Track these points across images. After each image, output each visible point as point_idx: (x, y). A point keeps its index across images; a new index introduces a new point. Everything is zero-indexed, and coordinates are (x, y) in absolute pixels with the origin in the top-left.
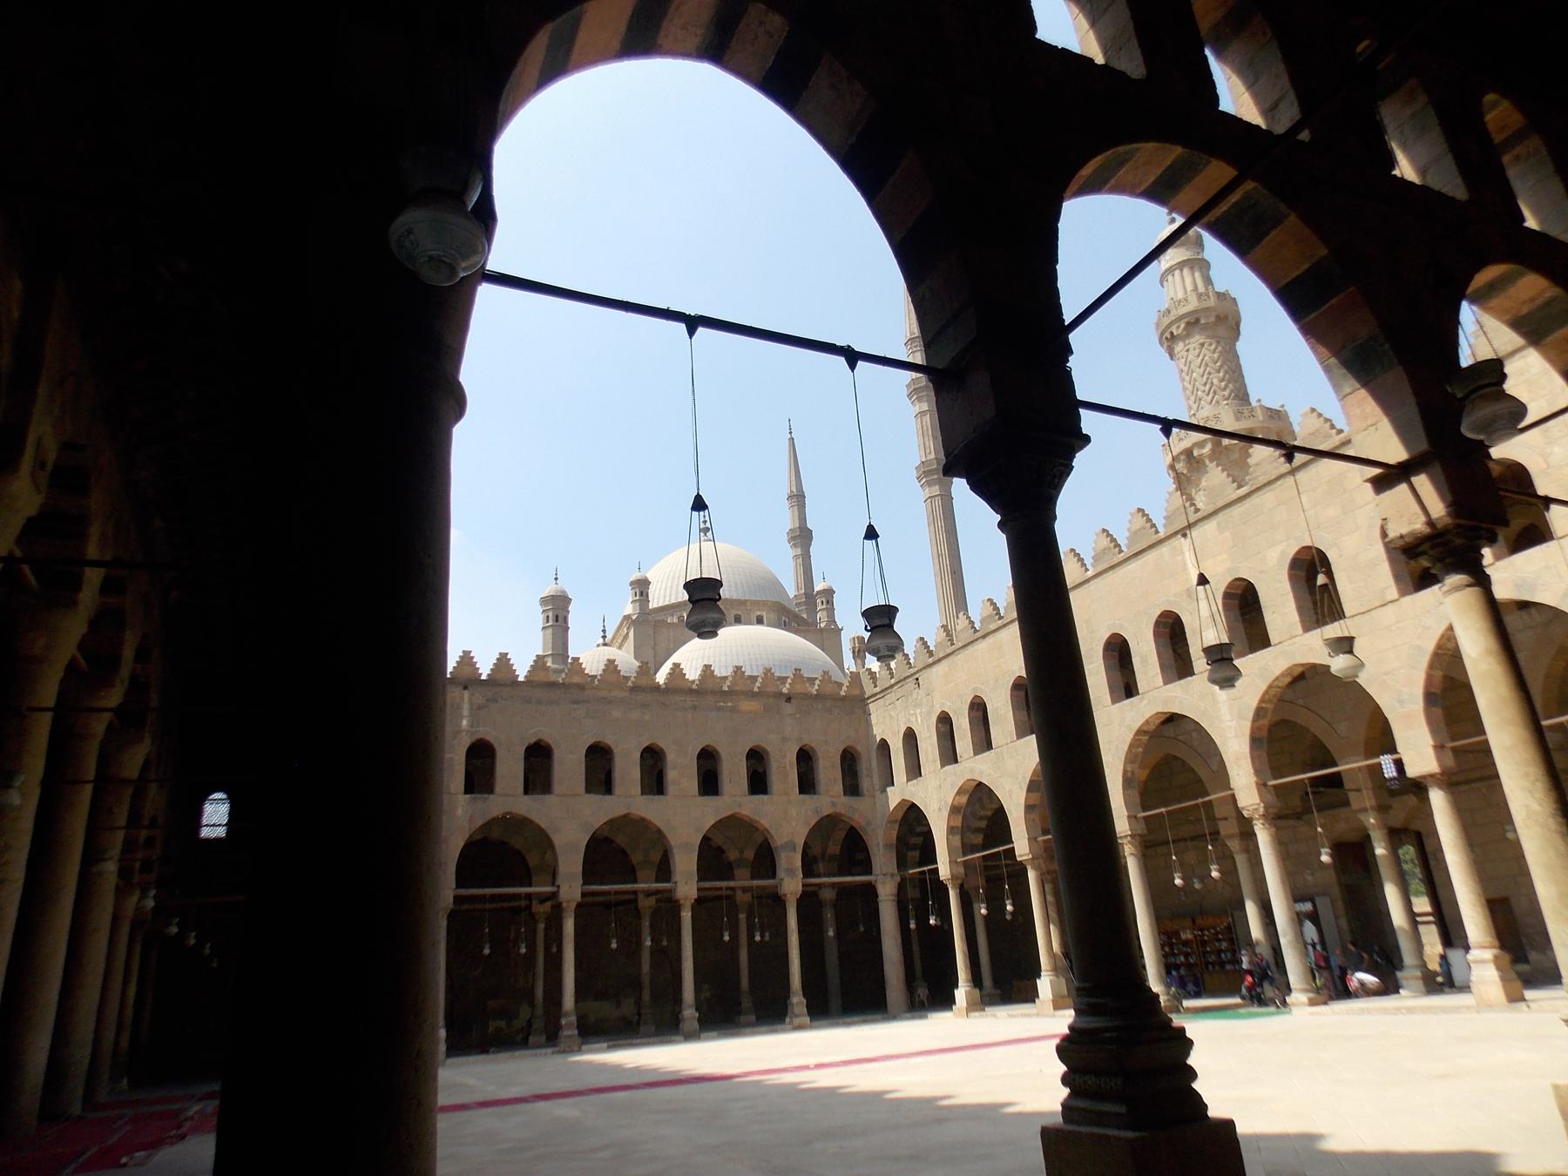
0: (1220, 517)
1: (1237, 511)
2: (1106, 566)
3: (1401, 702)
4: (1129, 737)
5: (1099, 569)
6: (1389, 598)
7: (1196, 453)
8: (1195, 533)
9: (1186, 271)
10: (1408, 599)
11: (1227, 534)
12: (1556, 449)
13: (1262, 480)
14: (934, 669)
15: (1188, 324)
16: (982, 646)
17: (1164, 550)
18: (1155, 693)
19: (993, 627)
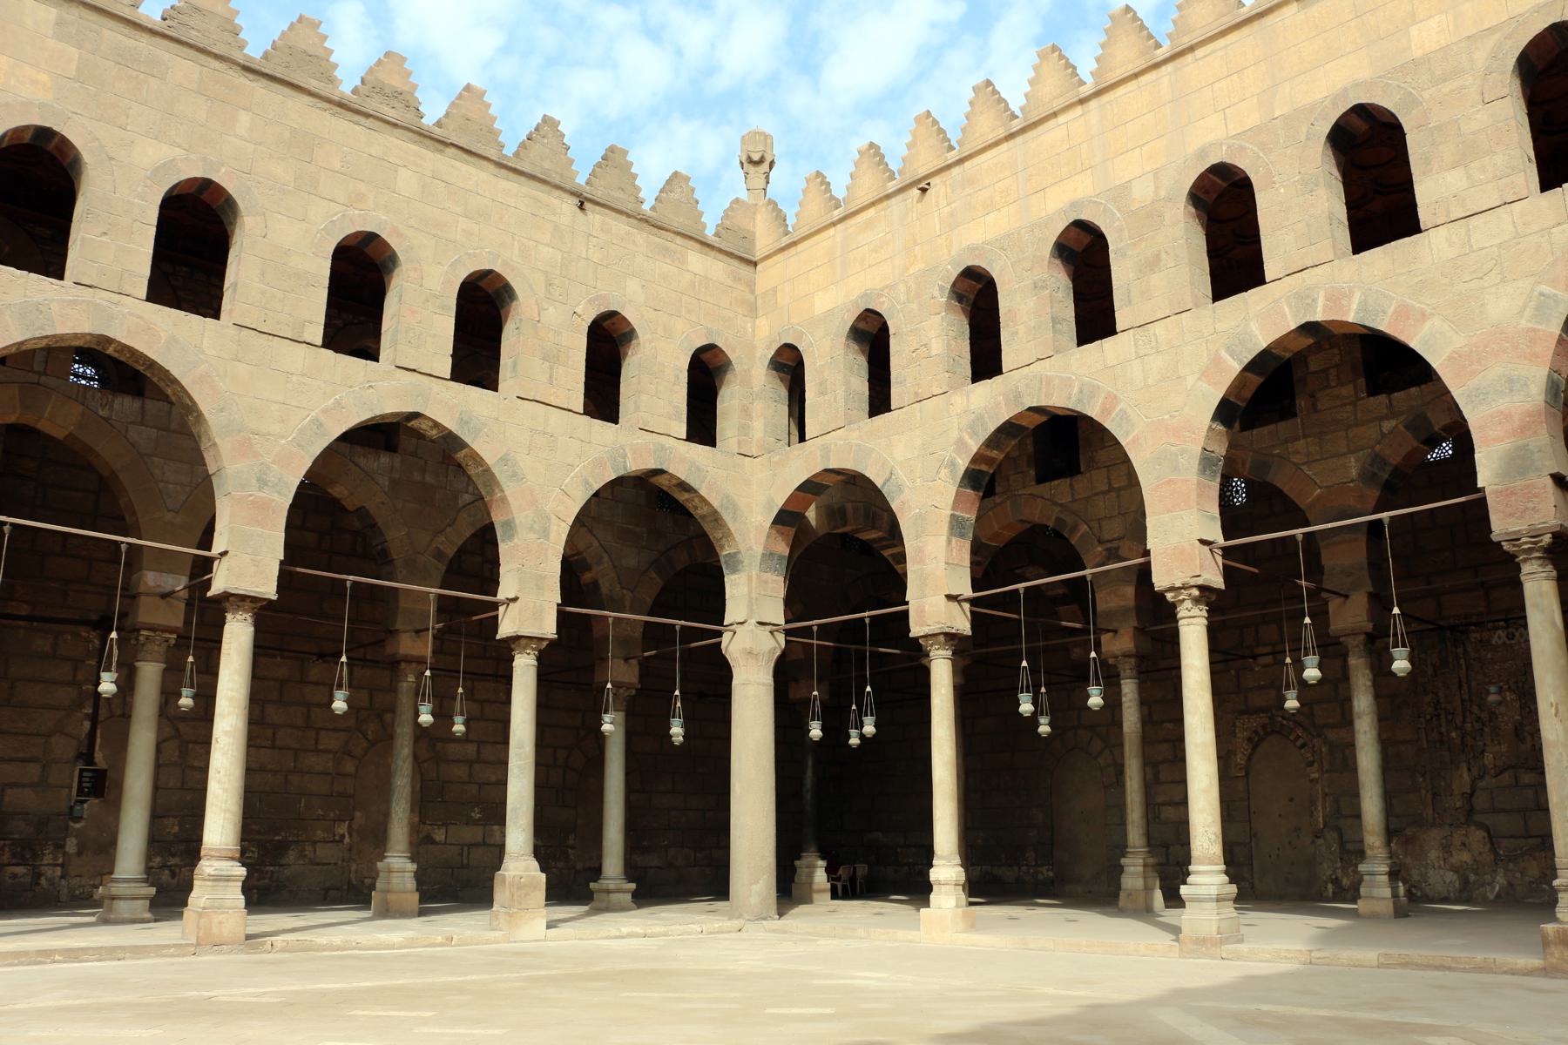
3: (263, 483)
10: (329, 353)
12: (551, 310)
13: (193, 36)
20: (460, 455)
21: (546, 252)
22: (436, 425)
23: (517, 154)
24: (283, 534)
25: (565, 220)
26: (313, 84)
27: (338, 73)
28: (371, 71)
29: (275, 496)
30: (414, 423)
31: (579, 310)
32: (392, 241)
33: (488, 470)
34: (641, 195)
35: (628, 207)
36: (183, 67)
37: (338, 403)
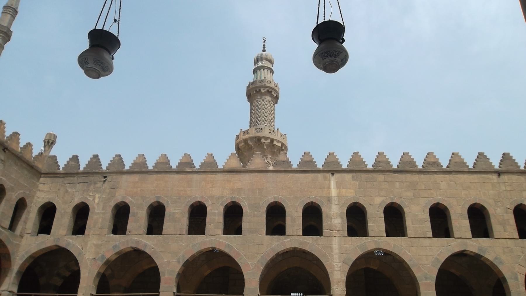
0: (354, 174)
1: (363, 176)
2: (282, 169)
4: (272, 255)
5: (278, 169)
6: (429, 236)
7: (263, 140)
8: (336, 176)
9: (269, 71)
10: (435, 239)
11: (357, 183)
12: (499, 209)
13: (381, 168)
14: (125, 177)
15: (268, 91)
16: (176, 176)
17: (320, 176)
18: (296, 237)
19: (187, 169)
20: (482, 259)
21: (492, 192)
22: (472, 252)
23: (474, 167)
24: (435, 292)
25: (495, 181)
26: (411, 169)
27: (417, 164)
28: (425, 160)
29: (430, 281)
30: (465, 252)
31: (508, 207)
32: (445, 204)
33: (492, 263)
34: (519, 165)
35: (515, 170)
36: (380, 177)
37: (441, 252)
